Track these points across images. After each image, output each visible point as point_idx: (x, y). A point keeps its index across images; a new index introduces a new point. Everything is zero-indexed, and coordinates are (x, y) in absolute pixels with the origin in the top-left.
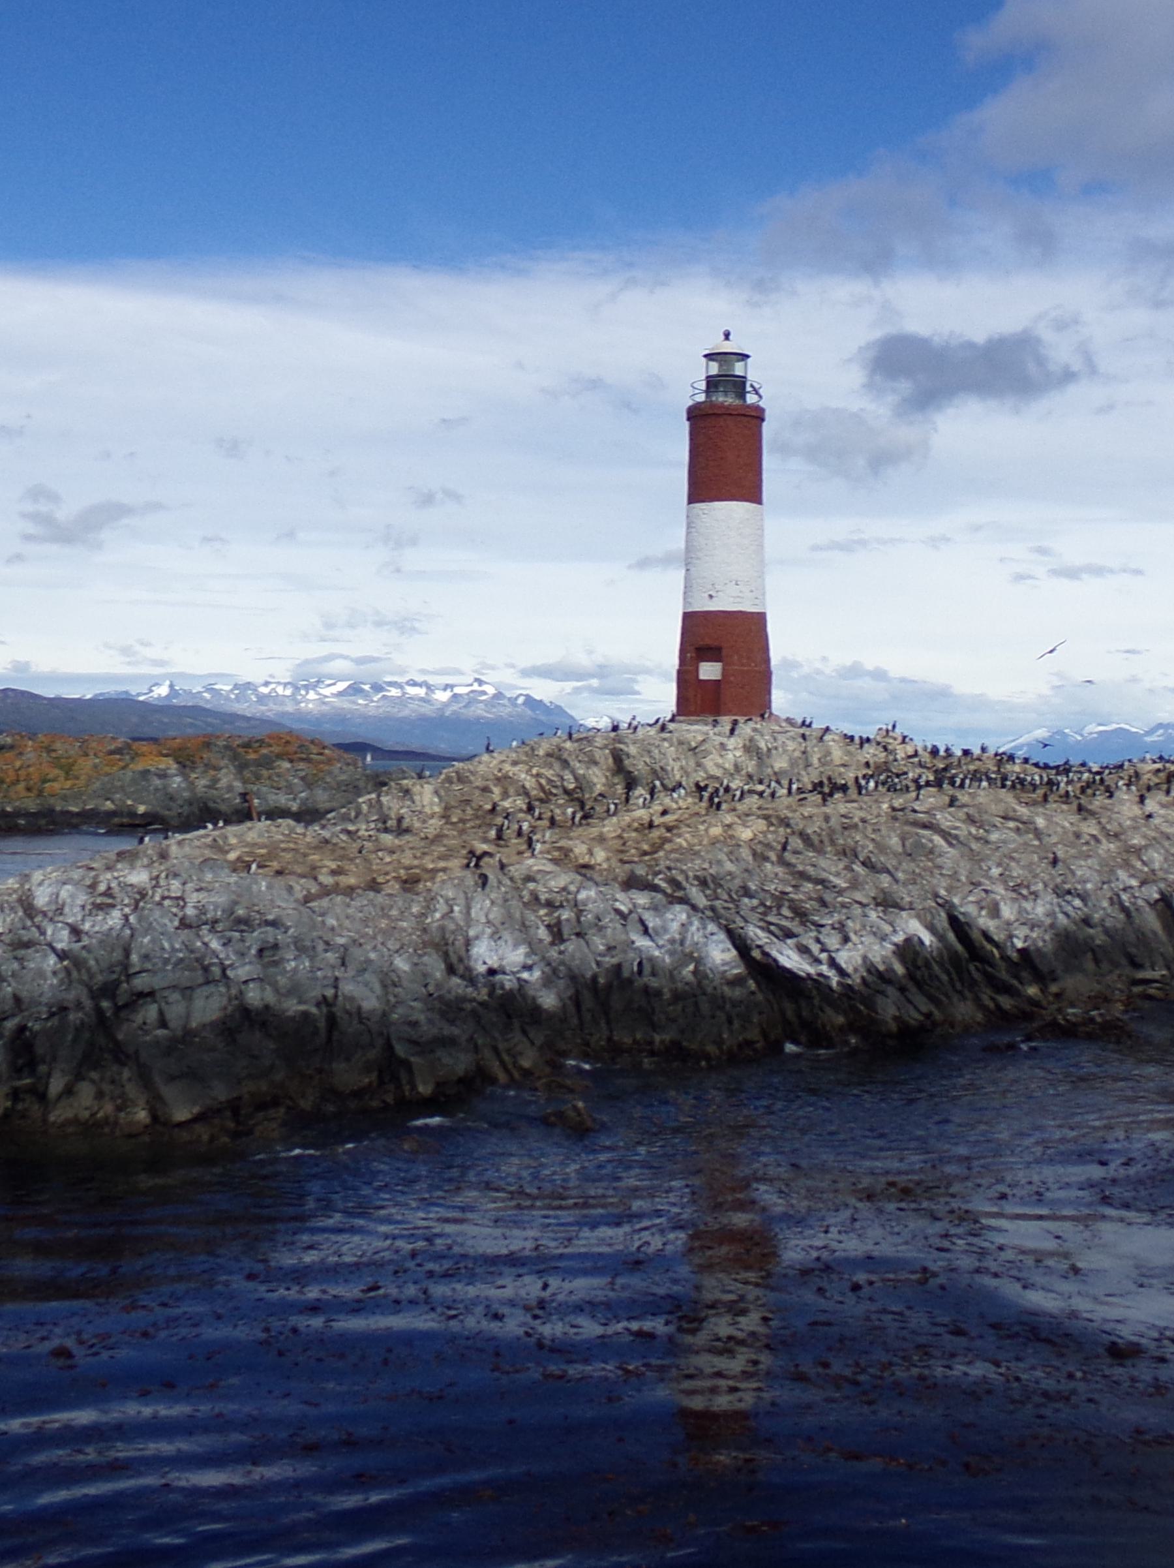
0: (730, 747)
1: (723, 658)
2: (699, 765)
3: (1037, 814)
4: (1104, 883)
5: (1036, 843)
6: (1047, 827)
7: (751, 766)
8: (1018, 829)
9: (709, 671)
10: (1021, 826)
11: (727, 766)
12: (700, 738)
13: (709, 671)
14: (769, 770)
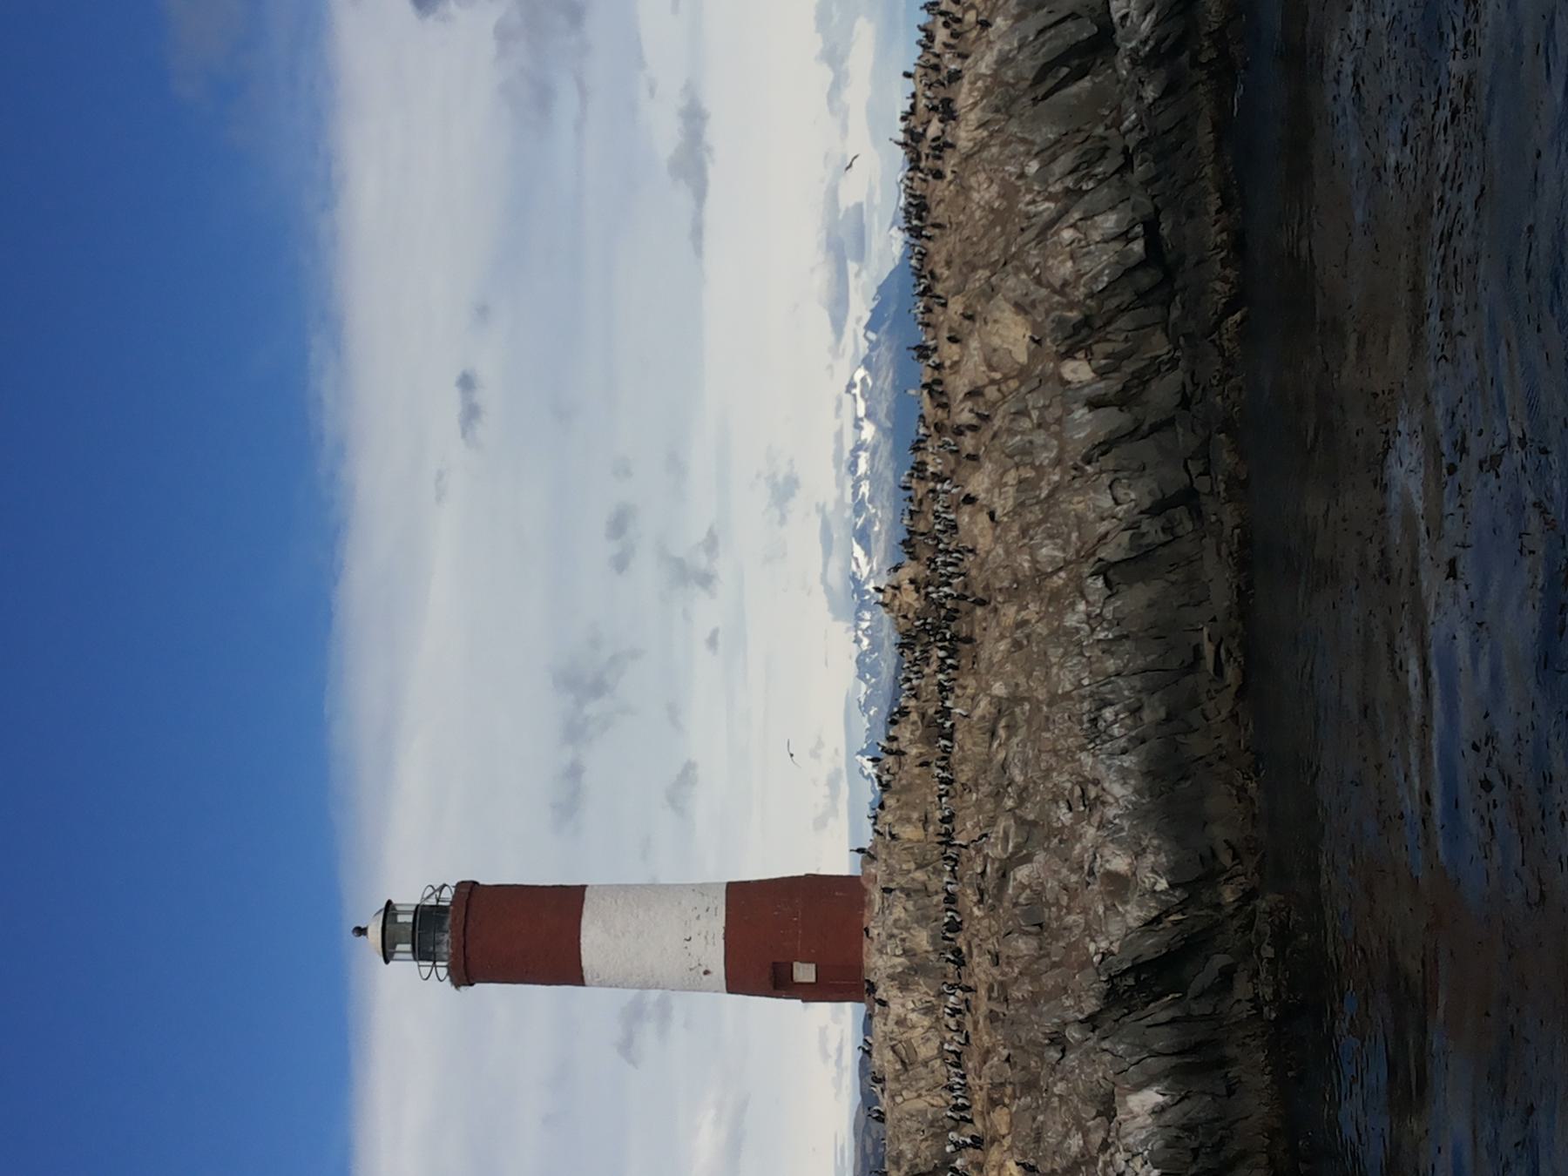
0: (901, 1011)
1: (783, 938)
2: (925, 1064)
5: (1027, 707)
6: (1007, 685)
7: (923, 991)
8: (1007, 727)
9: (805, 973)
10: (1003, 723)
12: (889, 1055)
13: (805, 973)
14: (932, 957)
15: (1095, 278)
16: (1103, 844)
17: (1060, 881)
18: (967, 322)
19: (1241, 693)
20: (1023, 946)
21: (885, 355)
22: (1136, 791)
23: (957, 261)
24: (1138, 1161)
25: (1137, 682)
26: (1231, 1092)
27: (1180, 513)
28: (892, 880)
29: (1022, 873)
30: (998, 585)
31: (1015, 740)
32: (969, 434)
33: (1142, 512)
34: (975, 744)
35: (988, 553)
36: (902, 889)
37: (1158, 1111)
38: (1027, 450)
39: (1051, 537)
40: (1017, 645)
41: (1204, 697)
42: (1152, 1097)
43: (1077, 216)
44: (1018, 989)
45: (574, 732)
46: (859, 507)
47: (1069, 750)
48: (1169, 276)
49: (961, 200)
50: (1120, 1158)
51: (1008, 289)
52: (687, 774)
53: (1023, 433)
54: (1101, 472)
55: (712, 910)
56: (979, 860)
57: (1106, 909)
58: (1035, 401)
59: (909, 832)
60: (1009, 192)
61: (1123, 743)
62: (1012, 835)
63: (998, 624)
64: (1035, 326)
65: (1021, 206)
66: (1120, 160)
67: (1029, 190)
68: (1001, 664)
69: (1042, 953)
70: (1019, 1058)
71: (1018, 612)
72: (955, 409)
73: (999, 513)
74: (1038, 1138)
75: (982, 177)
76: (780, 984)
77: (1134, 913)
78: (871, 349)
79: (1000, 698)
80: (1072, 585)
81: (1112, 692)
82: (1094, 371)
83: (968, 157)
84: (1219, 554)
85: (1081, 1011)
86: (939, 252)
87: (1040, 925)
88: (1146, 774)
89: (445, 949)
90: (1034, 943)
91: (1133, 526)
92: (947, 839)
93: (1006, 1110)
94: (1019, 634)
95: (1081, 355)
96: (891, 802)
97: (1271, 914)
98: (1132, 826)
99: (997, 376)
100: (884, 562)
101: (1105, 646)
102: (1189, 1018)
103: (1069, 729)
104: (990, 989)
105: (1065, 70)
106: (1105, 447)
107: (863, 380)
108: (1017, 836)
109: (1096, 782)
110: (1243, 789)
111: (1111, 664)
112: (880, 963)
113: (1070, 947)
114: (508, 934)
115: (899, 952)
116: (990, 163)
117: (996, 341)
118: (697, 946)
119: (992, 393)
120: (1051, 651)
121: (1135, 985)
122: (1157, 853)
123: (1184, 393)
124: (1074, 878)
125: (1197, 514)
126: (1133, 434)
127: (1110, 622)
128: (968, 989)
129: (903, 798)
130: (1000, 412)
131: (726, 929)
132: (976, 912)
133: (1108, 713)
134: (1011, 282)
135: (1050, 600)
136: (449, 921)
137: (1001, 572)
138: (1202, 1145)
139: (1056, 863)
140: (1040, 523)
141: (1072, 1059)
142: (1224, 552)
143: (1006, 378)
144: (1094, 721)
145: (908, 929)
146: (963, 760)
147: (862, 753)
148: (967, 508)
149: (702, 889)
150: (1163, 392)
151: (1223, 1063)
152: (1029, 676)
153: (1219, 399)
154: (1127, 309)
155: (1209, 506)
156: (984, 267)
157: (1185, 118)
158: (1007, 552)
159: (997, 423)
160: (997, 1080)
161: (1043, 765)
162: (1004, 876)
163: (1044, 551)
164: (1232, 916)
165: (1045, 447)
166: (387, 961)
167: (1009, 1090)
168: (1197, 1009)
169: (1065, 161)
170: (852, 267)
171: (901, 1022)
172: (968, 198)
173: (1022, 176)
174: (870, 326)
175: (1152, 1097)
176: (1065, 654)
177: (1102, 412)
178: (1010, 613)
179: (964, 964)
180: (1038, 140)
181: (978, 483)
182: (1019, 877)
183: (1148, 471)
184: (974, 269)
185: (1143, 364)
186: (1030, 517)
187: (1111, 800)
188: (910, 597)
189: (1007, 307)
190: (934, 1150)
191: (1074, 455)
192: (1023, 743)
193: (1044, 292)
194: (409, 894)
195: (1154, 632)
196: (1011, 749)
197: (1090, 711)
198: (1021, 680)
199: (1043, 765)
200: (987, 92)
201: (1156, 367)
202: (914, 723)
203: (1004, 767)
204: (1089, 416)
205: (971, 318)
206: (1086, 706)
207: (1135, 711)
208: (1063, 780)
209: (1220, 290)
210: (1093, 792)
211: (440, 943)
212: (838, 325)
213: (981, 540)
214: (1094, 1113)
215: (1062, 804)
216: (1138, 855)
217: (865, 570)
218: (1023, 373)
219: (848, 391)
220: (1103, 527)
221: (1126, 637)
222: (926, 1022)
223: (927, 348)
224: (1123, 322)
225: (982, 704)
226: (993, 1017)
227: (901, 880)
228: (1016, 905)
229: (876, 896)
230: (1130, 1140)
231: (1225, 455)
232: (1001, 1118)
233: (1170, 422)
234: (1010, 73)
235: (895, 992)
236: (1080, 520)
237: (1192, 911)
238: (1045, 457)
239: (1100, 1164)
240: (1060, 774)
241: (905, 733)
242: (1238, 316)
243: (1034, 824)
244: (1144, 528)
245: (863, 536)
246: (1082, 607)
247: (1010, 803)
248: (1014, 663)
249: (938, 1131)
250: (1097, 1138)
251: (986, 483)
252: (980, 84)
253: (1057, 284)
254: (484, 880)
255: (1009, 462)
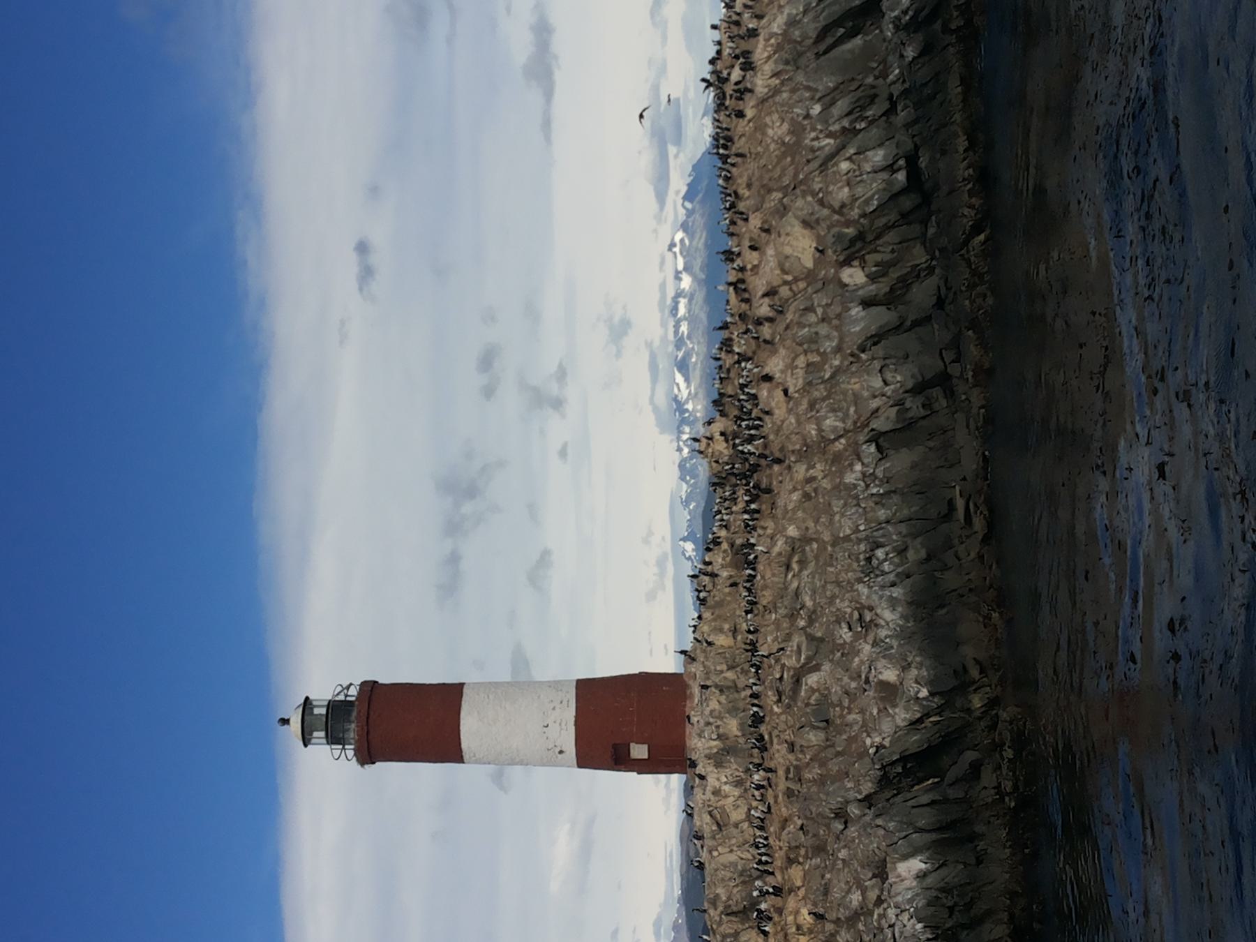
0: (717, 784)
1: (622, 723)
2: (736, 826)
3: (785, 529)
4: (858, 505)
5: (815, 546)
7: (734, 768)
8: (800, 562)
9: (639, 751)
10: (796, 558)
11: (736, 794)
12: (707, 818)
13: (639, 751)
14: (742, 740)
15: (867, 202)
16: (877, 659)
17: (842, 687)
18: (764, 235)
19: (986, 540)
20: (814, 738)
21: (699, 220)
22: (902, 617)
23: (756, 184)
24: (905, 916)
25: (903, 528)
26: (979, 862)
27: (936, 392)
28: (708, 679)
29: (812, 680)
30: (791, 448)
31: (806, 573)
32: (767, 324)
33: (906, 392)
34: (774, 575)
35: (783, 422)
36: (716, 686)
37: (921, 876)
38: (814, 339)
39: (834, 410)
40: (807, 496)
41: (956, 541)
42: (917, 864)
43: (852, 151)
44: (810, 772)
45: (453, 527)
46: (679, 342)
47: (849, 582)
48: (926, 199)
49: (759, 136)
50: (891, 913)
51: (797, 209)
52: (545, 558)
53: (810, 326)
54: (873, 359)
55: (565, 702)
56: (778, 668)
57: (879, 711)
58: (820, 300)
59: (722, 640)
60: (797, 130)
61: (892, 577)
62: (804, 648)
63: (792, 479)
64: (819, 239)
65: (807, 141)
66: (886, 105)
67: (814, 129)
68: (794, 510)
69: (829, 744)
70: (811, 828)
71: (807, 470)
72: (755, 304)
73: (791, 390)
74: (826, 892)
75: (775, 117)
76: (619, 760)
77: (901, 715)
78: (688, 216)
79: (793, 538)
80: (850, 449)
81: (883, 536)
82: (867, 276)
83: (763, 101)
84: (968, 426)
85: (860, 792)
86: (742, 175)
87: (827, 721)
88: (910, 604)
89: (352, 735)
90: (822, 735)
91: (899, 403)
92: (753, 647)
93: (800, 867)
94: (808, 488)
95: (856, 263)
96: (707, 615)
97: (1011, 723)
98: (900, 645)
99: (789, 278)
100: (700, 386)
101: (877, 499)
102: (945, 800)
103: (850, 565)
104: (788, 771)
105: (842, 30)
106: (876, 339)
107: (682, 241)
108: (808, 650)
109: (871, 609)
110: (988, 617)
111: (882, 514)
112: (700, 744)
113: (851, 740)
114: (402, 723)
115: (714, 736)
116: (782, 106)
117: (788, 250)
118: (553, 731)
119: (784, 292)
120: (834, 502)
121: (901, 772)
122: (919, 667)
123: (939, 298)
124: (853, 685)
125: (950, 394)
126: (898, 329)
127: (881, 480)
128: (769, 770)
129: (717, 612)
130: (792, 308)
131: (577, 717)
132: (776, 709)
133: (880, 553)
134: (800, 203)
135: (833, 462)
136: (354, 714)
137: (794, 438)
138: (956, 904)
139: (840, 673)
140: (824, 399)
141: (852, 831)
142: (972, 426)
143: (796, 280)
144: (869, 560)
145: (721, 718)
146: (765, 587)
147: (684, 539)
148: (766, 385)
149: (556, 685)
150: (922, 294)
151: (972, 838)
152: (817, 521)
153: (967, 302)
154: (893, 226)
155: (961, 388)
156: (776, 190)
157: (937, 74)
158: (799, 422)
159: (790, 316)
160: (793, 844)
161: (828, 593)
162: (797, 681)
163: (828, 422)
164: (980, 719)
165: (828, 337)
166: (306, 745)
167: (803, 851)
168: (953, 793)
169: (842, 105)
170: (672, 150)
171: (716, 792)
172: (764, 134)
173: (807, 116)
174: (688, 197)
175: (917, 864)
176: (845, 505)
177: (874, 310)
178: (800, 471)
179: (766, 749)
180: (820, 88)
181: (775, 365)
182: (810, 681)
183: (910, 359)
184: (770, 191)
185: (905, 271)
186: (816, 394)
187: (883, 623)
188: (720, 446)
189: (796, 222)
190: (744, 894)
191: (851, 345)
192: (812, 575)
193: (826, 212)
194: (323, 692)
195: (916, 488)
196: (803, 579)
197: (865, 551)
198: (811, 524)
199: (828, 593)
200: (779, 48)
201: (916, 274)
202: (725, 551)
203: (797, 593)
204: (863, 314)
205: (767, 231)
206: (862, 547)
207: (902, 552)
208: (844, 606)
209: (967, 216)
210: (868, 616)
211: (348, 730)
212: (661, 197)
213: (777, 411)
214: (870, 875)
215: (844, 625)
216: (905, 668)
217: (685, 393)
218: (810, 276)
219: (670, 249)
220: (875, 404)
221: (894, 492)
222: (737, 792)
223: (732, 253)
224: (891, 237)
225: (780, 543)
226: (789, 793)
227: (716, 679)
228: (807, 705)
229: (696, 690)
230: (899, 899)
231: (972, 348)
232: (796, 874)
233: (928, 319)
234: (797, 33)
235: (711, 768)
236: (856, 396)
237: (947, 714)
238: (828, 346)
239: (875, 917)
240: (842, 600)
241: (718, 559)
242: (982, 237)
243: (821, 640)
244: (908, 405)
245: (683, 366)
246: (858, 467)
247: (802, 623)
248: (804, 511)
249: (746, 878)
250: (873, 895)
251: (781, 366)
252: (773, 41)
253: (837, 205)
254: (383, 680)
255: (800, 349)
